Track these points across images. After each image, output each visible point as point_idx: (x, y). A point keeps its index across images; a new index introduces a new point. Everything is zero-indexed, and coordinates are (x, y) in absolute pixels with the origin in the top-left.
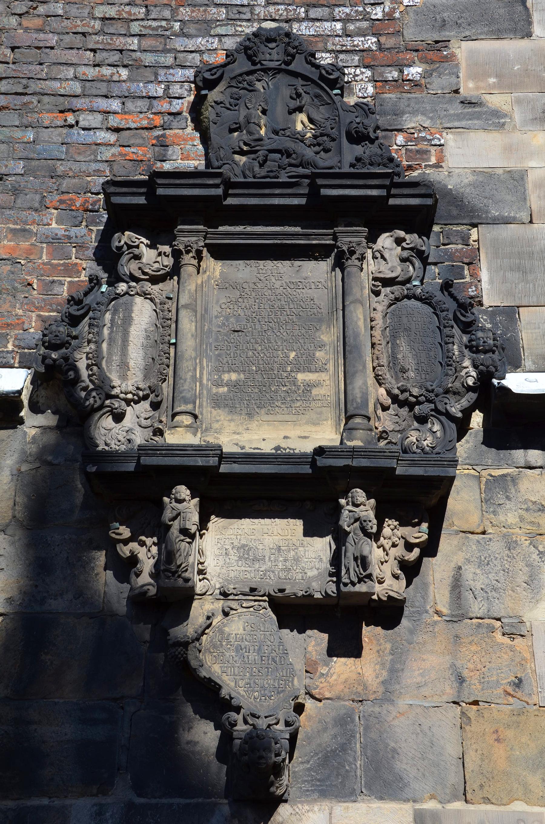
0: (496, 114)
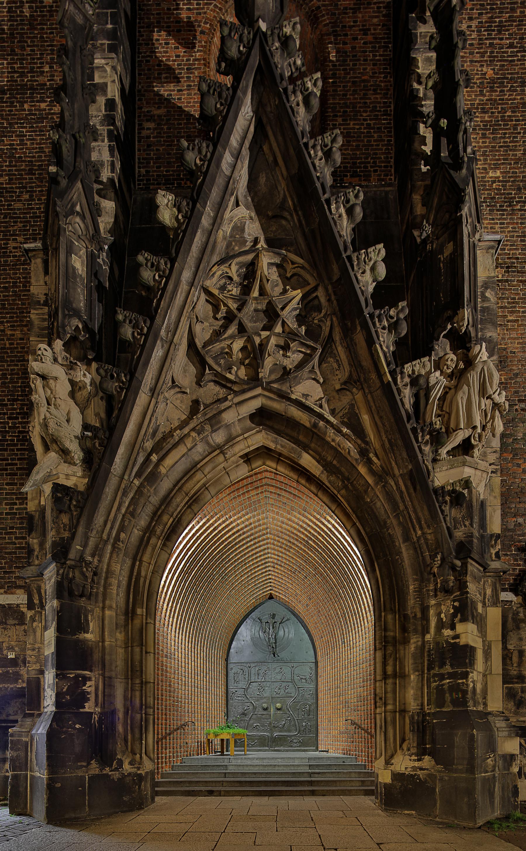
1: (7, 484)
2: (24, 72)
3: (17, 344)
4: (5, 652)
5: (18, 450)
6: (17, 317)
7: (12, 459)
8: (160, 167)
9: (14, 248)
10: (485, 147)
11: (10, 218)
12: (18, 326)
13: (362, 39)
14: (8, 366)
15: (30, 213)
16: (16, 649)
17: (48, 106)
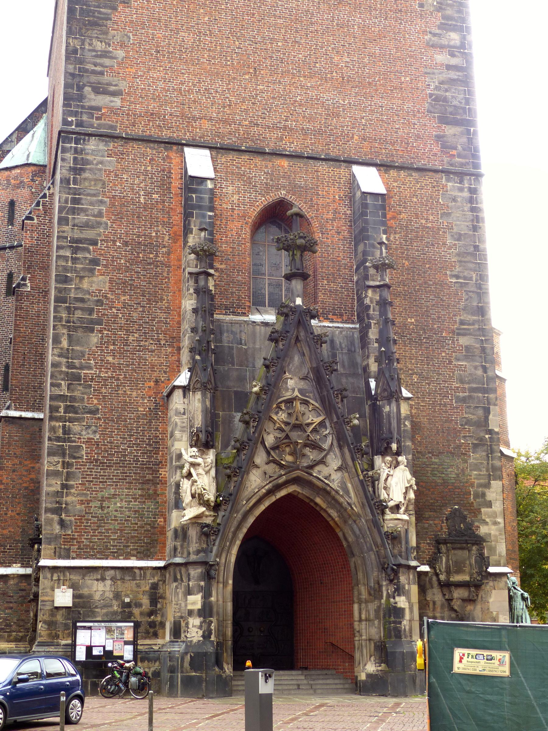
0: (487, 522)
1: (126, 489)
3: (134, 400)
4: (123, 598)
5: (133, 467)
6: (134, 383)
7: (130, 473)
8: (222, 299)
9: (133, 340)
10: (406, 305)
11: (131, 322)
12: (135, 389)
13: (337, 237)
14: (128, 413)
16: (131, 596)
17: (154, 256)
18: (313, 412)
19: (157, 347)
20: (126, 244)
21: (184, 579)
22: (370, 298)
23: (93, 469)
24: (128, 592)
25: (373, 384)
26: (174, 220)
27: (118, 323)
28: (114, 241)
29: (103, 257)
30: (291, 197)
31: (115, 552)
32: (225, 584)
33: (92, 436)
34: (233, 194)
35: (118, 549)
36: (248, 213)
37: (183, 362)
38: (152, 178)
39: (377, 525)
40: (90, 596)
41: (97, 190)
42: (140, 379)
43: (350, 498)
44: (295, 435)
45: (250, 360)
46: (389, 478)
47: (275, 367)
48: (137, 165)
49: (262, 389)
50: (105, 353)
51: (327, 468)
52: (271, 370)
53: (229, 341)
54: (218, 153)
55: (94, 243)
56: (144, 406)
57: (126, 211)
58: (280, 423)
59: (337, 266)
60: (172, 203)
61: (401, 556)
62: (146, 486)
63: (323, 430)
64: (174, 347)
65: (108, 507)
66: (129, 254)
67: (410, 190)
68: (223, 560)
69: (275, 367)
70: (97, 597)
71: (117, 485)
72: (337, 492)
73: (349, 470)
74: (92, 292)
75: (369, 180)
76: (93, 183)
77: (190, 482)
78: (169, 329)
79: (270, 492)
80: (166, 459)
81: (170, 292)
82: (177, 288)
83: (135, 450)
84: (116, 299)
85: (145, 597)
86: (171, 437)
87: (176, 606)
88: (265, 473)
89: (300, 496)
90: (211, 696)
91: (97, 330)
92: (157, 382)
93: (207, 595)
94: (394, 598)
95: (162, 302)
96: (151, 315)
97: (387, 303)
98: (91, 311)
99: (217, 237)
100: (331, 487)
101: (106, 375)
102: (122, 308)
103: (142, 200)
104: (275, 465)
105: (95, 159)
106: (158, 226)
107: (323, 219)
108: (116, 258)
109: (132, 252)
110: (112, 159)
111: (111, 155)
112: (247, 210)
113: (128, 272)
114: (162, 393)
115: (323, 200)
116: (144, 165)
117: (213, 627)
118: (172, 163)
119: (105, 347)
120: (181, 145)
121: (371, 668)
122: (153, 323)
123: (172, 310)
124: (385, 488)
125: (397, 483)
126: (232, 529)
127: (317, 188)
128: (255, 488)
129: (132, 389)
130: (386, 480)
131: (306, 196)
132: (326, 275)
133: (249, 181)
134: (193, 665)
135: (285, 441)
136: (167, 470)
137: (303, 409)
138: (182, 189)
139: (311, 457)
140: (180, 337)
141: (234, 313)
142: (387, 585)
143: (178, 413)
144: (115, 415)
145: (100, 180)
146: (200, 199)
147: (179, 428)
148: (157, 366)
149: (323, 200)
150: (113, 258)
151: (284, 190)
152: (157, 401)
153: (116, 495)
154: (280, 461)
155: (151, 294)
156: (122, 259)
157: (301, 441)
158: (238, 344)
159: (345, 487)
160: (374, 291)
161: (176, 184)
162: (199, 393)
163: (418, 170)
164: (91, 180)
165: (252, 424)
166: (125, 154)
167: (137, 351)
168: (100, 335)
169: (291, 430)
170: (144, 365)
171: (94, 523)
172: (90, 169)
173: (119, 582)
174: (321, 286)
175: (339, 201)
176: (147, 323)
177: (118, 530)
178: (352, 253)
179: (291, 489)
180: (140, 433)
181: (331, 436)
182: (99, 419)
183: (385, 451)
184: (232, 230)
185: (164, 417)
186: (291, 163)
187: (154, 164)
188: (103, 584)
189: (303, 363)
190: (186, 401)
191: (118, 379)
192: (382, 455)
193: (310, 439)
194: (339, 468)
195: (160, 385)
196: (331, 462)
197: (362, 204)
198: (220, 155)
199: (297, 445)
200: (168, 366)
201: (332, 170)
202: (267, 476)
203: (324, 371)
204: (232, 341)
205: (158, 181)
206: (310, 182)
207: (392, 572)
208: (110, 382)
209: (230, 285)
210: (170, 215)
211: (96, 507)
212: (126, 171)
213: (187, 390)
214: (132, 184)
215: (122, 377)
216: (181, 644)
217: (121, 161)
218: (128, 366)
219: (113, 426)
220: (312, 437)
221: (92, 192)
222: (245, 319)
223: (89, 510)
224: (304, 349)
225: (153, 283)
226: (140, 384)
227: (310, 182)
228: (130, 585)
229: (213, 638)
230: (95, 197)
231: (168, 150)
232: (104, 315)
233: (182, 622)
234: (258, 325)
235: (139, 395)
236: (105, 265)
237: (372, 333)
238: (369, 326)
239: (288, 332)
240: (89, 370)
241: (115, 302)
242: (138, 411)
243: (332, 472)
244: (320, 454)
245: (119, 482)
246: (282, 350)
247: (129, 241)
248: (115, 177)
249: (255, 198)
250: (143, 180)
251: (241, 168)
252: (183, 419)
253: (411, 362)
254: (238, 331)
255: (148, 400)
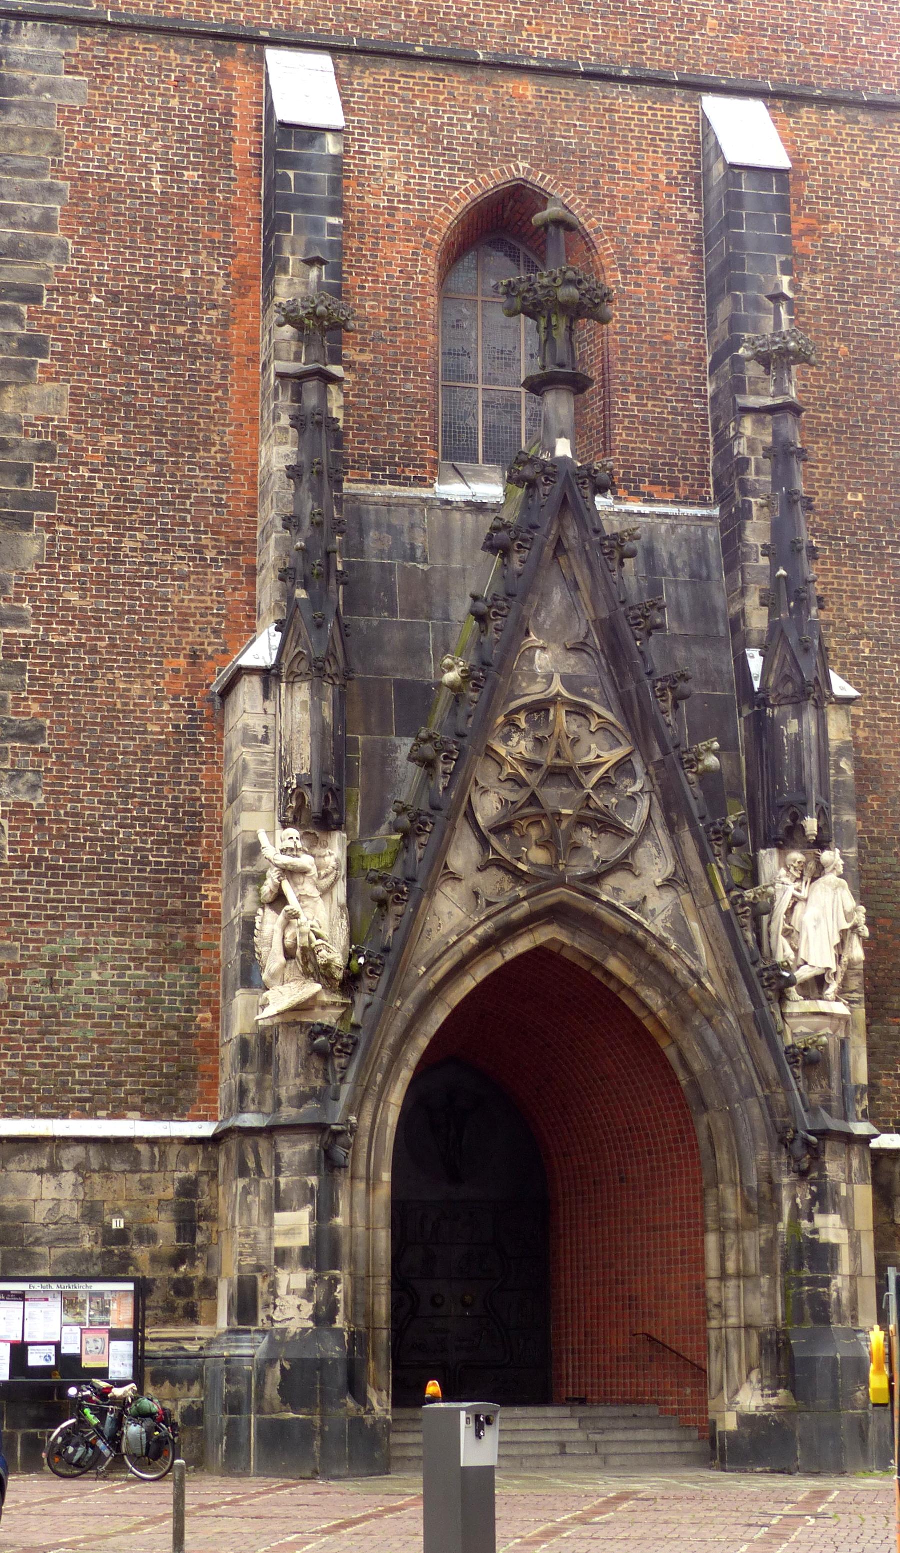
1: (115, 934)
2: (150, 276)
3: (135, 705)
4: (107, 1219)
5: (134, 879)
6: (135, 661)
7: (125, 894)
8: (363, 443)
9: (133, 550)
10: (842, 457)
11: (126, 501)
12: (138, 676)
13: (661, 282)
14: (120, 739)
15: (157, 496)
16: (127, 1213)
17: (188, 331)
18: (600, 735)
19: (196, 566)
20: (114, 299)
21: (265, 1170)
22: (749, 440)
23: (30, 883)
24: (121, 1204)
25: (755, 663)
26: (241, 238)
27: (93, 506)
28: (84, 293)
29: (56, 333)
30: (543, 178)
31: (87, 1100)
32: (372, 1182)
33: (26, 799)
34: (393, 169)
35: (95, 1092)
36: (432, 218)
37: (263, 606)
38: (182, 128)
39: (765, 1028)
40: (22, 1214)
41: (40, 159)
42: (151, 649)
43: (697, 958)
44: (553, 796)
45: (438, 600)
46: (799, 908)
47: (502, 619)
48: (143, 94)
49: (467, 676)
50: (59, 582)
51: (635, 882)
52: (492, 626)
53: (382, 551)
54: (353, 63)
55: (32, 296)
56: (162, 720)
57: (115, 215)
58: (516, 765)
59: (663, 356)
60: (235, 193)
61: (828, 1109)
62: (165, 929)
63: (627, 782)
64: (241, 568)
65: (69, 983)
66: (122, 326)
67: (853, 160)
68: (367, 1121)
69: (502, 619)
70: (39, 1215)
71: (91, 926)
72: (662, 943)
73: (693, 886)
74: (27, 425)
75: (747, 133)
76: (28, 141)
77: (281, 918)
78: (225, 521)
79: (489, 944)
80: (219, 858)
81: (230, 425)
82: (248, 412)
83: (137, 834)
84: (88, 443)
85: (163, 1216)
86: (231, 801)
87: (244, 1240)
88: (476, 895)
89: (567, 954)
90: (336, 1472)
91: (38, 524)
92: (194, 657)
93: (325, 1211)
94: (811, 1219)
95: (209, 451)
96: (181, 483)
97: (792, 453)
98: (23, 474)
99: (352, 280)
100: (647, 931)
101: (63, 640)
102: (103, 465)
103: (157, 186)
104: (501, 874)
105: (34, 78)
106: (197, 253)
107: (627, 235)
108: (89, 336)
109: (131, 321)
110: (78, 78)
111: (76, 67)
112: (428, 212)
113: (119, 372)
114: (208, 686)
115: (626, 186)
116: (160, 95)
117: (339, 1295)
118: (234, 90)
119: (61, 567)
120: (256, 42)
121: (751, 1399)
122: (184, 504)
123: (234, 472)
124: (788, 934)
125: (818, 921)
126: (391, 1040)
127: (611, 154)
128: (451, 932)
129: (130, 676)
130: (791, 911)
131: (582, 175)
132: (635, 379)
133: (434, 136)
134: (289, 1392)
135: (527, 811)
136: (220, 886)
137: (574, 728)
138: (260, 156)
139: (596, 853)
140: (255, 542)
141: (395, 479)
142: (793, 1185)
143: (249, 739)
144: (85, 744)
145: (49, 133)
146: (307, 182)
147: (251, 776)
148: (194, 615)
149: (626, 186)
150: (81, 335)
151: (524, 158)
152: (194, 706)
153: (89, 950)
154: (515, 862)
155: (179, 429)
156: (104, 337)
157: (570, 812)
158: (405, 559)
159: (680, 929)
160: (759, 423)
161: (245, 142)
162: (306, 686)
163: (874, 106)
164: (22, 134)
165: (441, 767)
166: (112, 65)
167: (143, 578)
168: (47, 536)
169: (543, 783)
170: (161, 614)
171: (31, 1024)
172: (21, 106)
173: (96, 1178)
174: (620, 410)
175: (668, 189)
176: (169, 503)
177: (94, 1041)
178: (702, 323)
179: (543, 935)
180: (150, 790)
181: (647, 797)
182: (45, 753)
183: (787, 837)
184: (390, 264)
185: (213, 749)
186: (544, 89)
187: (188, 92)
188: (54, 1182)
189: (573, 608)
190: (270, 706)
191: (94, 651)
192: (780, 848)
193: (592, 805)
194: (668, 880)
195: (202, 665)
196: (647, 865)
197: (728, 195)
198: (358, 69)
199: (560, 821)
200: (225, 617)
201: (650, 108)
202: (482, 902)
203: (628, 629)
204: (390, 552)
205: (198, 137)
206: (594, 140)
207: (806, 1151)
208: (73, 659)
209: (384, 405)
210: (228, 224)
211: (36, 982)
212: (114, 110)
213: (273, 679)
214: (130, 144)
215: (104, 644)
216: (258, 1337)
217: (102, 83)
218: (119, 615)
219: (82, 773)
220: (598, 801)
221: (27, 164)
222: (425, 493)
223: (18, 989)
224: (577, 572)
225: (186, 400)
226: (150, 663)
227: (594, 140)
228: (125, 1185)
229: (340, 1322)
230: (35, 177)
231: (224, 54)
232: (57, 482)
233: (260, 1280)
234: (458, 509)
235: (148, 690)
236: (59, 353)
237: (754, 531)
238: (745, 512)
239: (535, 527)
240: (18, 627)
241: (87, 450)
242: (145, 732)
243: (649, 891)
244: (618, 844)
245: (97, 918)
246: (520, 575)
247: (122, 293)
248: (85, 126)
249: (451, 181)
250: (158, 133)
251: (413, 102)
252: (262, 754)
253: (855, 605)
254: (407, 524)
255: (172, 706)
